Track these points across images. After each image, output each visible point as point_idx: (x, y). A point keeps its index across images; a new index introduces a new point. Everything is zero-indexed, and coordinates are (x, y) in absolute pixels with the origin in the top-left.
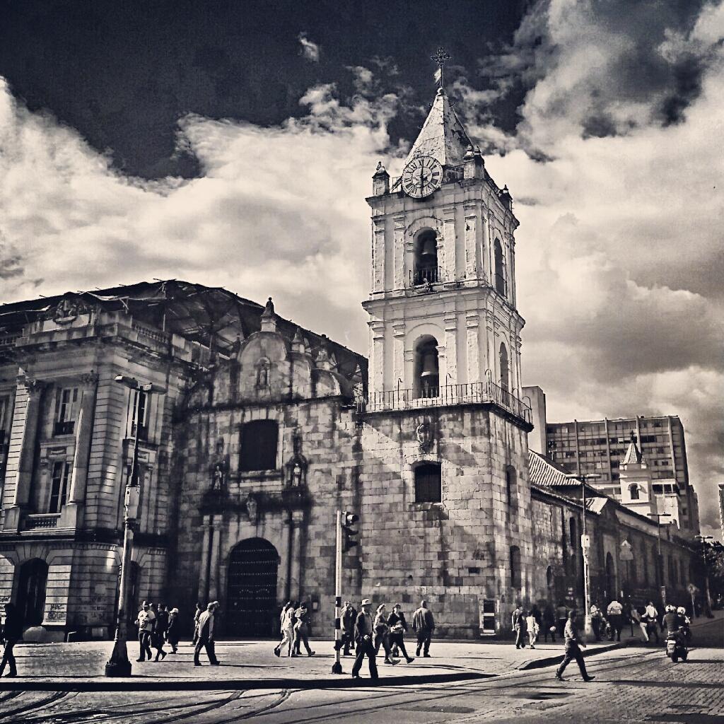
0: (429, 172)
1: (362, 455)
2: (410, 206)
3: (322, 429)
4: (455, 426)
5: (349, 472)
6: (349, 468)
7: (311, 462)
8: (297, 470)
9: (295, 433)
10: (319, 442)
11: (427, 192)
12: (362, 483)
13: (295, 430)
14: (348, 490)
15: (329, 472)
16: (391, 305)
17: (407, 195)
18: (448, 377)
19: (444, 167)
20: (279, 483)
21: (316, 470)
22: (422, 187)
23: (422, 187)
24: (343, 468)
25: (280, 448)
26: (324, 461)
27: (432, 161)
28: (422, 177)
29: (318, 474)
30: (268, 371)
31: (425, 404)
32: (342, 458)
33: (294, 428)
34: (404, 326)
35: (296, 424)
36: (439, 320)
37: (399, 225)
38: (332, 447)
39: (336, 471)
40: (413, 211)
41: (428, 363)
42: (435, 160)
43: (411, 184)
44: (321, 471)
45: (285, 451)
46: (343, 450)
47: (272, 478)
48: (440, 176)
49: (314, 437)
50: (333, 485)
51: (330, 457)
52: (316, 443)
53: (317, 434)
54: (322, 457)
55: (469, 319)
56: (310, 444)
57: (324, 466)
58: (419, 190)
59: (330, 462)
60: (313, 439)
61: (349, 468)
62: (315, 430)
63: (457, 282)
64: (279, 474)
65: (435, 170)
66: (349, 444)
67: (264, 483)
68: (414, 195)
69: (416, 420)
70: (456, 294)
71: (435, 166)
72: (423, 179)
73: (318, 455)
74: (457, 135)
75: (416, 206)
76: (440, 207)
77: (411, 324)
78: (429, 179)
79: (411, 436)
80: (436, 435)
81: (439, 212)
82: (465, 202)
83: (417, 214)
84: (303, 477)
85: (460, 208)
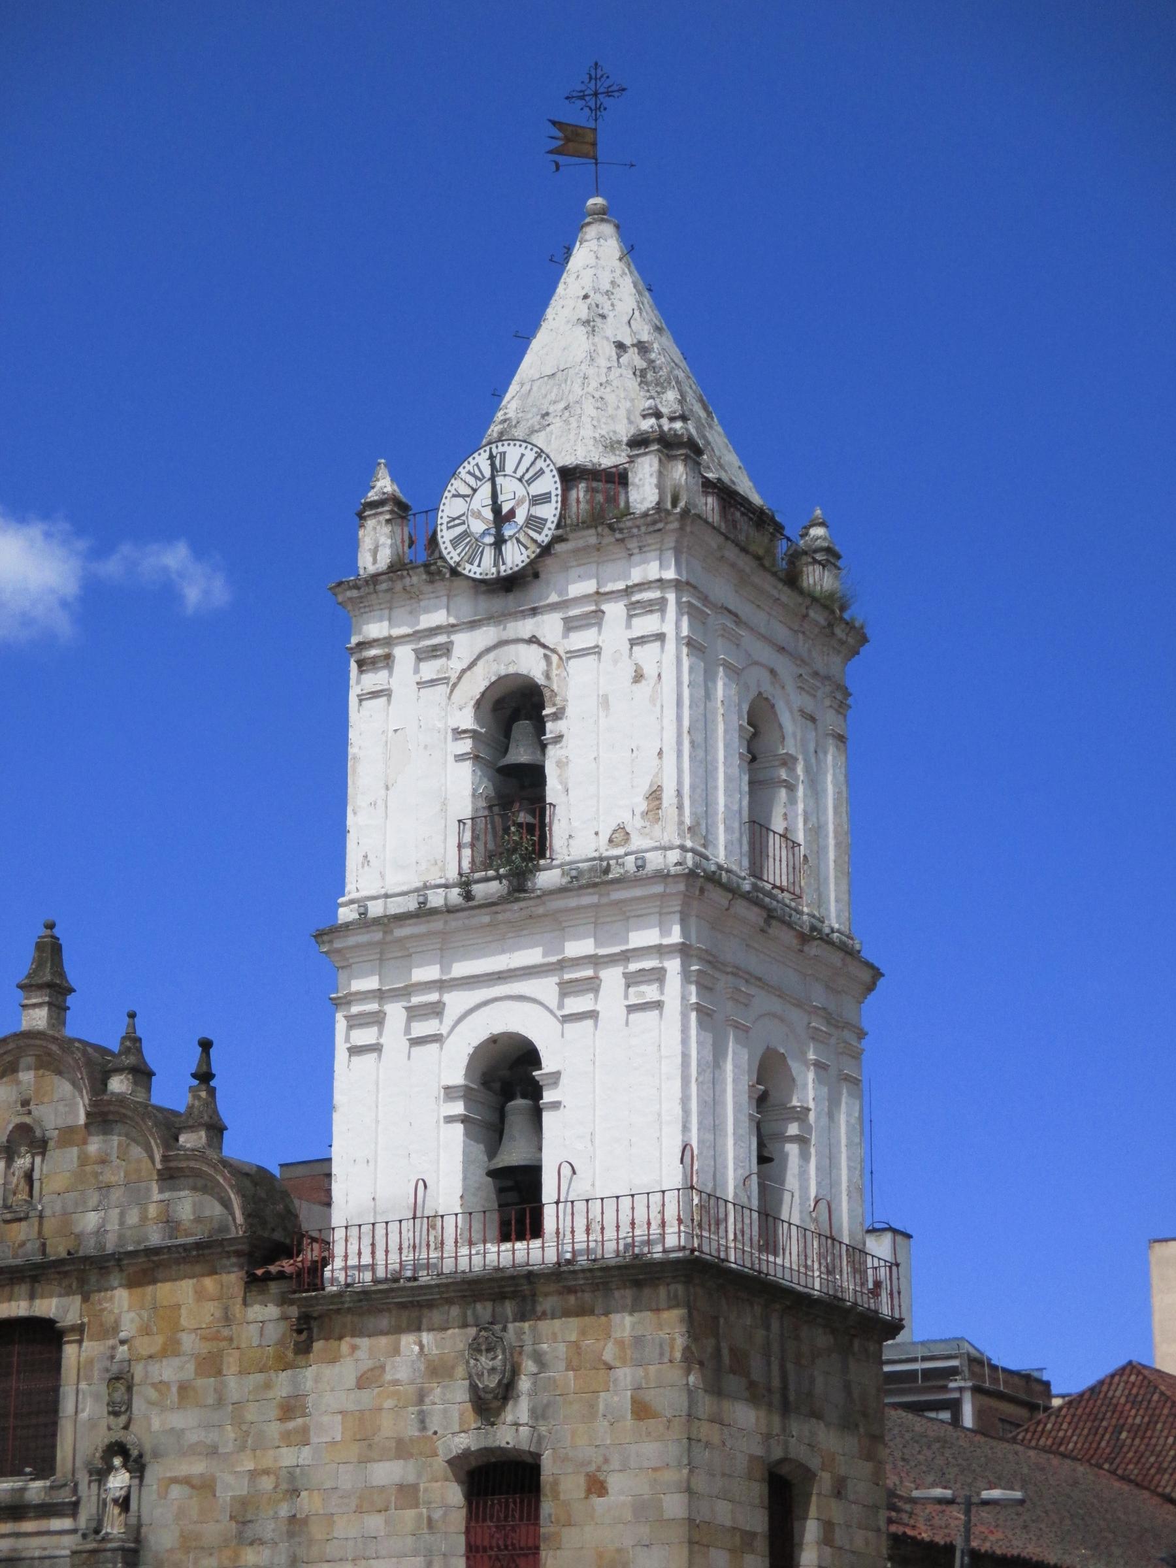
0: (521, 491)
1: (305, 1431)
2: (466, 607)
3: (189, 1342)
4: (583, 1333)
5: (267, 1483)
6: (266, 1472)
7: (156, 1455)
8: (119, 1481)
9: (112, 1357)
10: (184, 1388)
11: (515, 557)
12: (305, 1521)
13: (113, 1348)
14: (262, 1542)
15: (204, 1487)
16: (400, 940)
17: (455, 572)
18: (566, 1171)
19: (569, 476)
20: (66, 1523)
21: (175, 1480)
22: (499, 542)
23: (499, 542)
24: (254, 1474)
25: (68, 1406)
26: (192, 1451)
27: (530, 456)
28: (496, 509)
29: (176, 1491)
30: (38, 1159)
31: (521, 1256)
32: (250, 1440)
33: (111, 1342)
34: (436, 1010)
35: (116, 1329)
36: (546, 988)
37: (430, 669)
38: (220, 1402)
39: (231, 1486)
40: (473, 625)
41: (516, 1123)
42: (540, 453)
43: (466, 534)
44: (186, 1481)
45: (84, 1416)
46: (251, 1413)
47: (47, 1510)
48: (553, 504)
49: (169, 1371)
50: (216, 1528)
51: (213, 1437)
52: (174, 1389)
53: (176, 1362)
54: (193, 1437)
55: (631, 980)
56: (153, 1394)
57: (197, 1467)
58: (489, 555)
59: (212, 1452)
60: (165, 1378)
61: (266, 1472)
62: (171, 1349)
63: (601, 859)
64: (65, 1496)
65: (538, 488)
66: (270, 1395)
67: (28, 1526)
68: (473, 570)
69: (469, 1313)
70: (594, 899)
71: (541, 472)
72: (501, 518)
73: (178, 1434)
74: (633, 357)
75: (488, 604)
76: (554, 607)
77: (456, 1002)
78: (520, 517)
79: (453, 1367)
80: (529, 1366)
81: (549, 626)
82: (628, 591)
83: (486, 635)
84: (133, 1505)
85: (615, 610)
